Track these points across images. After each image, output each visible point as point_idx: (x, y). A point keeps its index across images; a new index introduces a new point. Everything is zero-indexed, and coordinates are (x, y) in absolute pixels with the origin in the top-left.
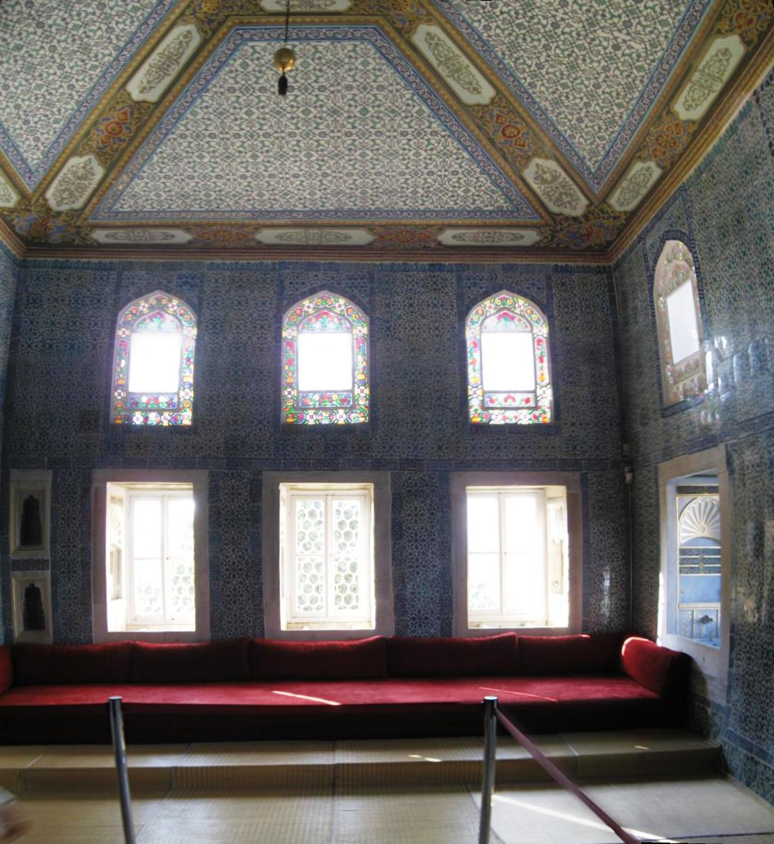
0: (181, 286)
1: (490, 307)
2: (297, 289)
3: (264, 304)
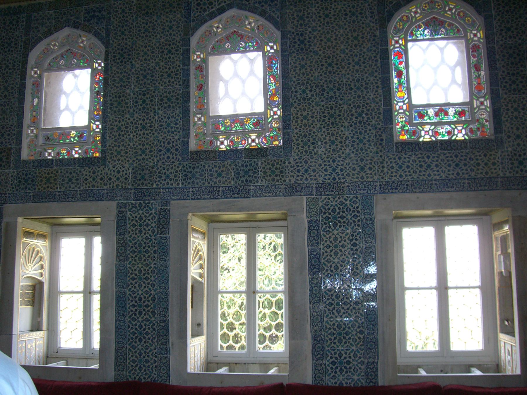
0: (89, 21)
1: (416, 13)
2: (205, 10)
3: (171, 28)
